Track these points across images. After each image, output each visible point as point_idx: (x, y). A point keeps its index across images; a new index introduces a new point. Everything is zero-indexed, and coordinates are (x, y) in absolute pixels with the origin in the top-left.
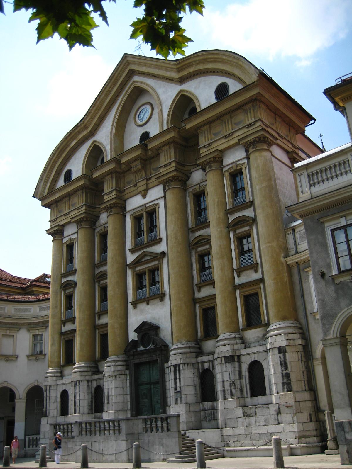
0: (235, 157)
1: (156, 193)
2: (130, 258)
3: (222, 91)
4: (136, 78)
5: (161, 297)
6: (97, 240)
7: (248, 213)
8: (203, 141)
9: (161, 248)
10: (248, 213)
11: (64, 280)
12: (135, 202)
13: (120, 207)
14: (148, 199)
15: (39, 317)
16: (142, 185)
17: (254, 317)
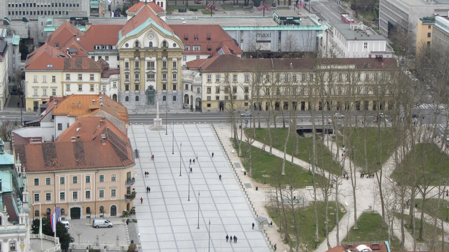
0: (175, 59)
1: (154, 59)
2: (147, 71)
3: (174, 45)
4: (151, 28)
5: (154, 81)
6: (135, 63)
7: (176, 71)
8: (169, 54)
9: (155, 71)
10: (176, 71)
11: (125, 71)
12: (148, 59)
13: (144, 59)
14: (151, 59)
15: (115, 78)
16: (151, 56)
17: (175, 88)
